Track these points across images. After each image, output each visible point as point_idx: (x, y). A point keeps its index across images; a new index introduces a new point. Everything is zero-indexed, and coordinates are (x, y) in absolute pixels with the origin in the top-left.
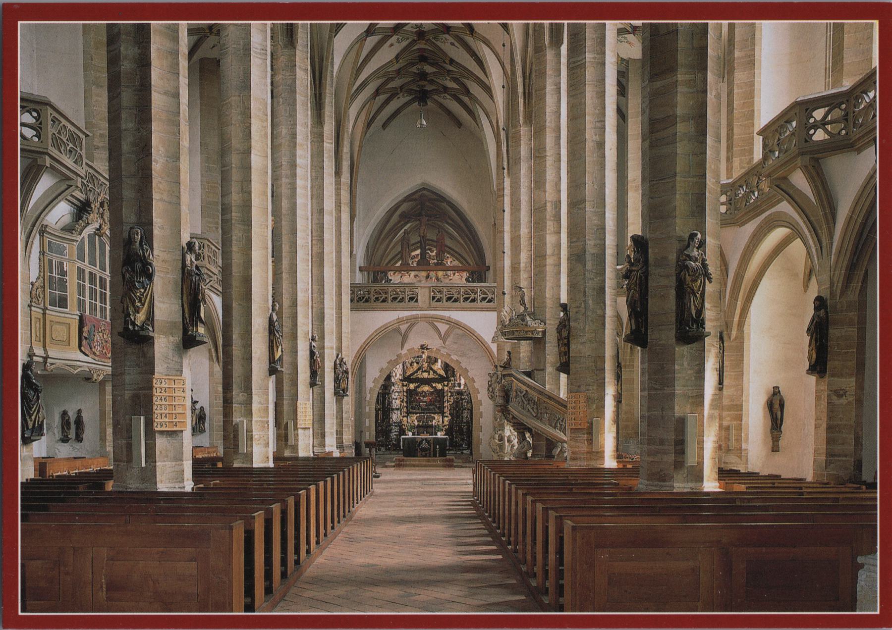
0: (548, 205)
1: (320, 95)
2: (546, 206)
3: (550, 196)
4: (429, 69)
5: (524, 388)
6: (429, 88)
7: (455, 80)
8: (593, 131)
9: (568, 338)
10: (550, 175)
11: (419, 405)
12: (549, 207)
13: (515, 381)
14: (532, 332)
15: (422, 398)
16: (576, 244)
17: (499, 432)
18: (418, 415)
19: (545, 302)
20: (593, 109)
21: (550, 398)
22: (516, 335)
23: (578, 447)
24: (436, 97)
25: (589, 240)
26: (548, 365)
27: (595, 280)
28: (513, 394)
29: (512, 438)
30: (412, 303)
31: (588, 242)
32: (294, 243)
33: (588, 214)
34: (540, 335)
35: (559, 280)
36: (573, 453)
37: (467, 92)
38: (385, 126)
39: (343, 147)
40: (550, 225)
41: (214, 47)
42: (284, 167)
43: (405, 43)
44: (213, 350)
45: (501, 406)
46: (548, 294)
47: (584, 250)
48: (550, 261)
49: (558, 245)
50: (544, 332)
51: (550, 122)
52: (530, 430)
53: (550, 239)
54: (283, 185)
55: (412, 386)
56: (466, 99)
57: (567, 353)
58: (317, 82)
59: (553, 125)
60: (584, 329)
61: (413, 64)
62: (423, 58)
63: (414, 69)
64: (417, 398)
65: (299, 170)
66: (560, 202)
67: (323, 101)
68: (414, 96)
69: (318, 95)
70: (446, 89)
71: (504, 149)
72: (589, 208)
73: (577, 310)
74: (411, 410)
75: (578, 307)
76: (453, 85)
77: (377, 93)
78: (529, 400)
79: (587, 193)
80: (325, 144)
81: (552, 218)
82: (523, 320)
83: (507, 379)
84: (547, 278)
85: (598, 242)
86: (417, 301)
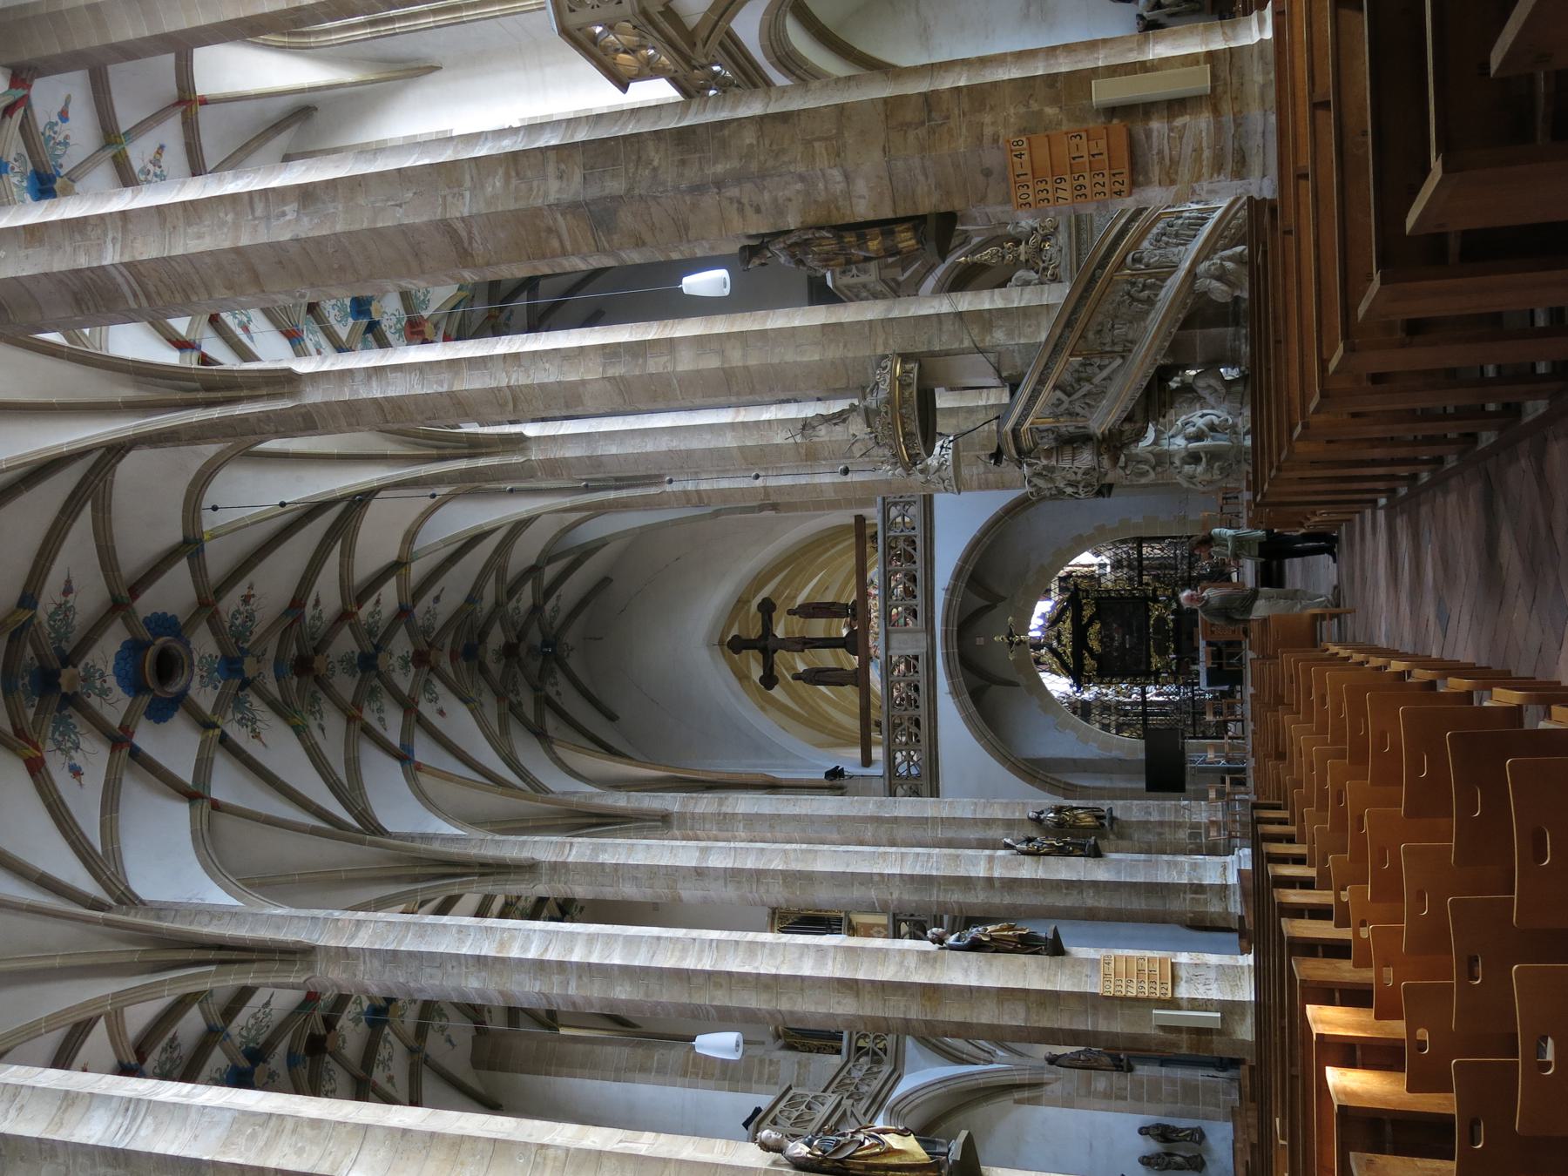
0: (611, 372)
1: (482, 865)
2: (614, 378)
3: (590, 372)
4: (496, 638)
5: (1046, 394)
6: (535, 637)
7: (513, 591)
8: (274, 223)
9: (840, 229)
10: (548, 375)
11: (1131, 648)
12: (616, 371)
13: (1030, 420)
14: (903, 386)
15: (1116, 644)
16: (565, 236)
17: (1177, 462)
18: (1152, 649)
19: (833, 363)
20: (226, 230)
21: (1069, 324)
22: (914, 426)
23: (1198, 151)
24: (557, 623)
25: (546, 194)
26: (988, 342)
27: (656, 163)
28: (1067, 426)
29: (1191, 430)
30: (921, 666)
31: (552, 199)
32: (711, 976)
33: (482, 208)
34: (913, 366)
35: (779, 331)
36: (1218, 167)
37: (534, 571)
38: (611, 717)
39: (616, 808)
40: (655, 365)
41: (450, 1041)
42: (545, 990)
43: (439, 687)
44: (1017, 1095)
45: (1099, 454)
46: (812, 356)
47: (573, 208)
48: (736, 358)
49: (699, 341)
50: (905, 358)
51: (441, 383)
52: (1163, 375)
53: (686, 362)
54: (582, 993)
55: (1090, 663)
56: (550, 572)
57: (885, 226)
58: (458, 870)
59: (446, 376)
60: (802, 178)
61: (483, 670)
62: (470, 652)
63: (495, 668)
64: (1115, 654)
65: (552, 955)
66: (604, 346)
67: (491, 861)
68: (554, 665)
69: (482, 870)
70: (536, 609)
71: (612, 495)
72: (463, 207)
73: (749, 211)
74: (1143, 667)
75: (741, 210)
76: (526, 596)
77: (540, 734)
78: (1079, 380)
79: (425, 218)
80: (570, 860)
81: (641, 361)
82: (877, 412)
83: (1026, 442)
84: (776, 360)
85: (551, 169)
86: (916, 658)
